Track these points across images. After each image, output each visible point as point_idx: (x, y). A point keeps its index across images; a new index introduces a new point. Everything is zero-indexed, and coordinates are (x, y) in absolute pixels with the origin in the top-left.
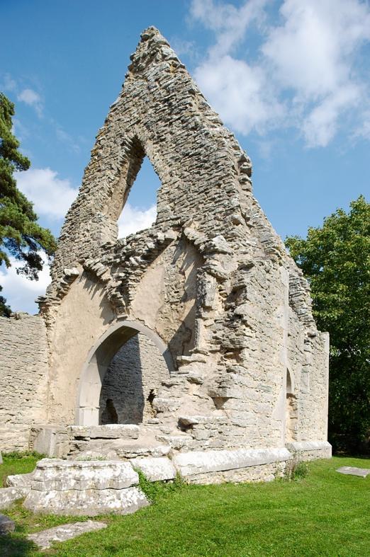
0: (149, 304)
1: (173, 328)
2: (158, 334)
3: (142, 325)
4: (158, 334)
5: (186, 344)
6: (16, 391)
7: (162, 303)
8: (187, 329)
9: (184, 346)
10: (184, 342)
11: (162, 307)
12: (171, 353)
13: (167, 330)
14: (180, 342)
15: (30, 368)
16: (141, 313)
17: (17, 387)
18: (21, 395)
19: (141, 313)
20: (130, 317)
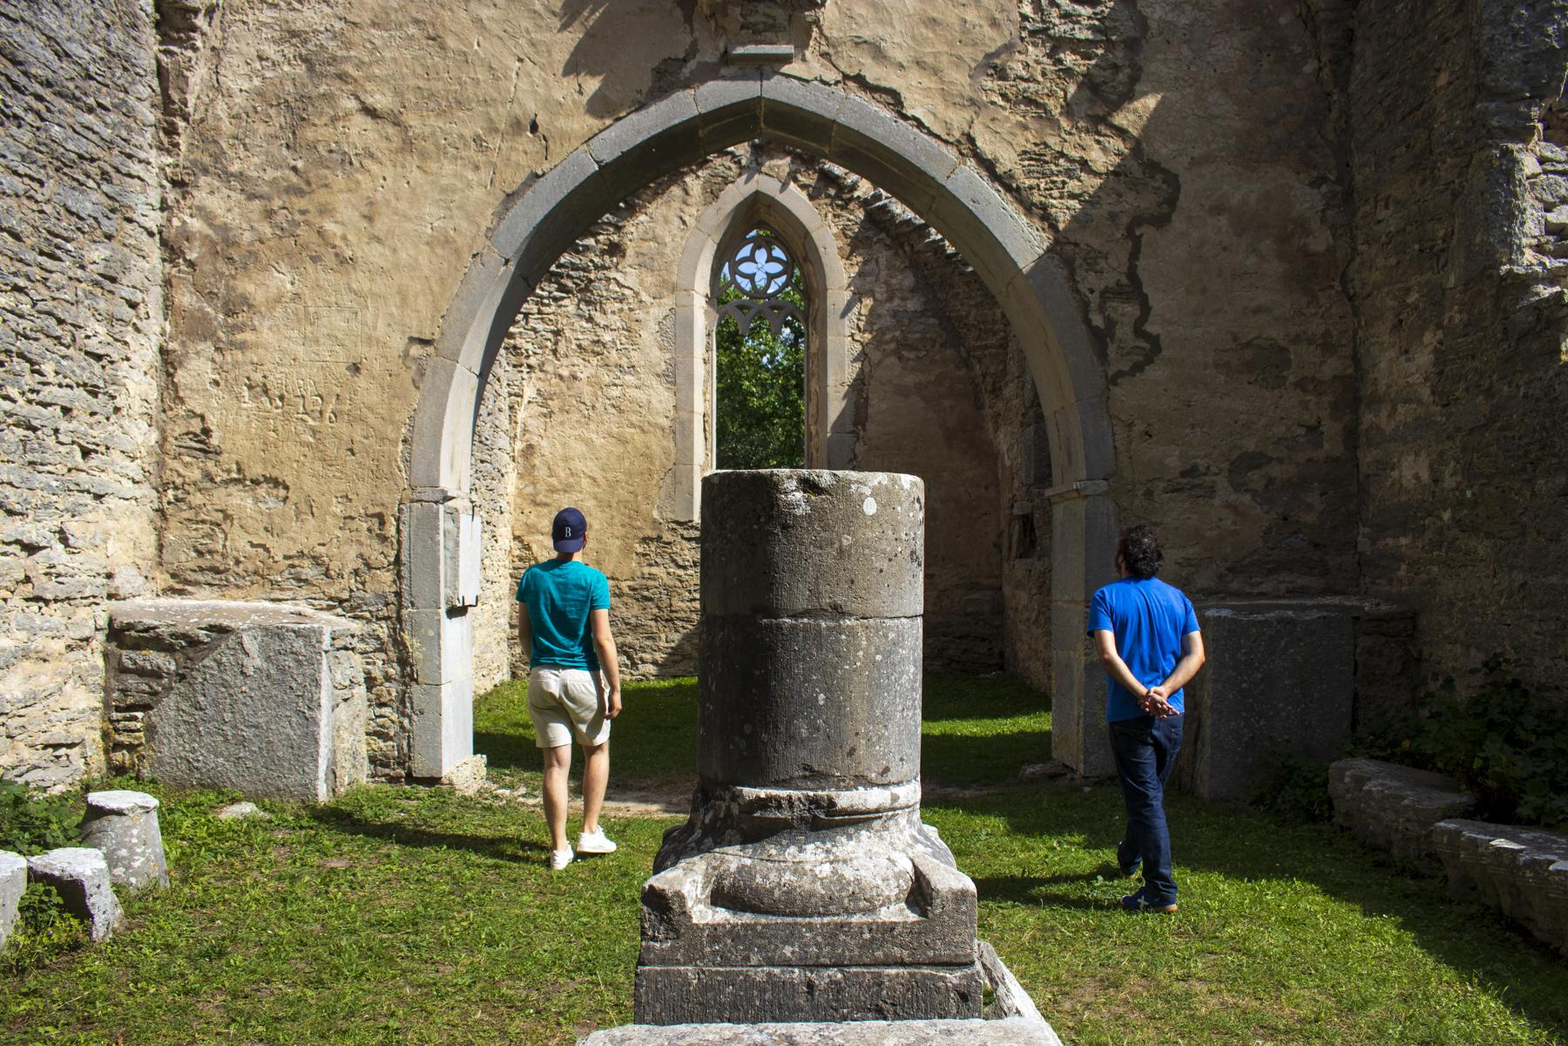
0: (932, 22)
1: (1075, 154)
2: (988, 166)
3: (887, 114)
4: (988, 166)
5: (1147, 232)
6: (46, 394)
7: (1010, 30)
8: (1153, 167)
9: (1137, 242)
10: (1137, 221)
11: (1008, 48)
12: (1069, 263)
13: (1038, 158)
14: (1113, 217)
15: (97, 254)
16: (878, 53)
17: (48, 368)
18: (63, 425)
19: (878, 53)
20: (809, 66)
